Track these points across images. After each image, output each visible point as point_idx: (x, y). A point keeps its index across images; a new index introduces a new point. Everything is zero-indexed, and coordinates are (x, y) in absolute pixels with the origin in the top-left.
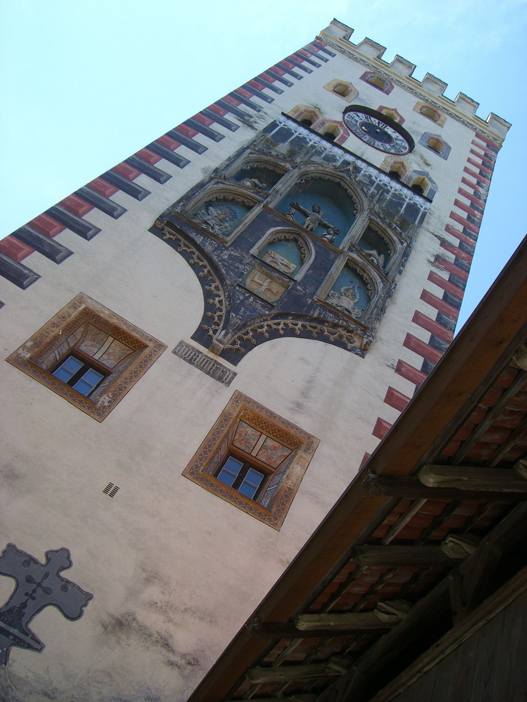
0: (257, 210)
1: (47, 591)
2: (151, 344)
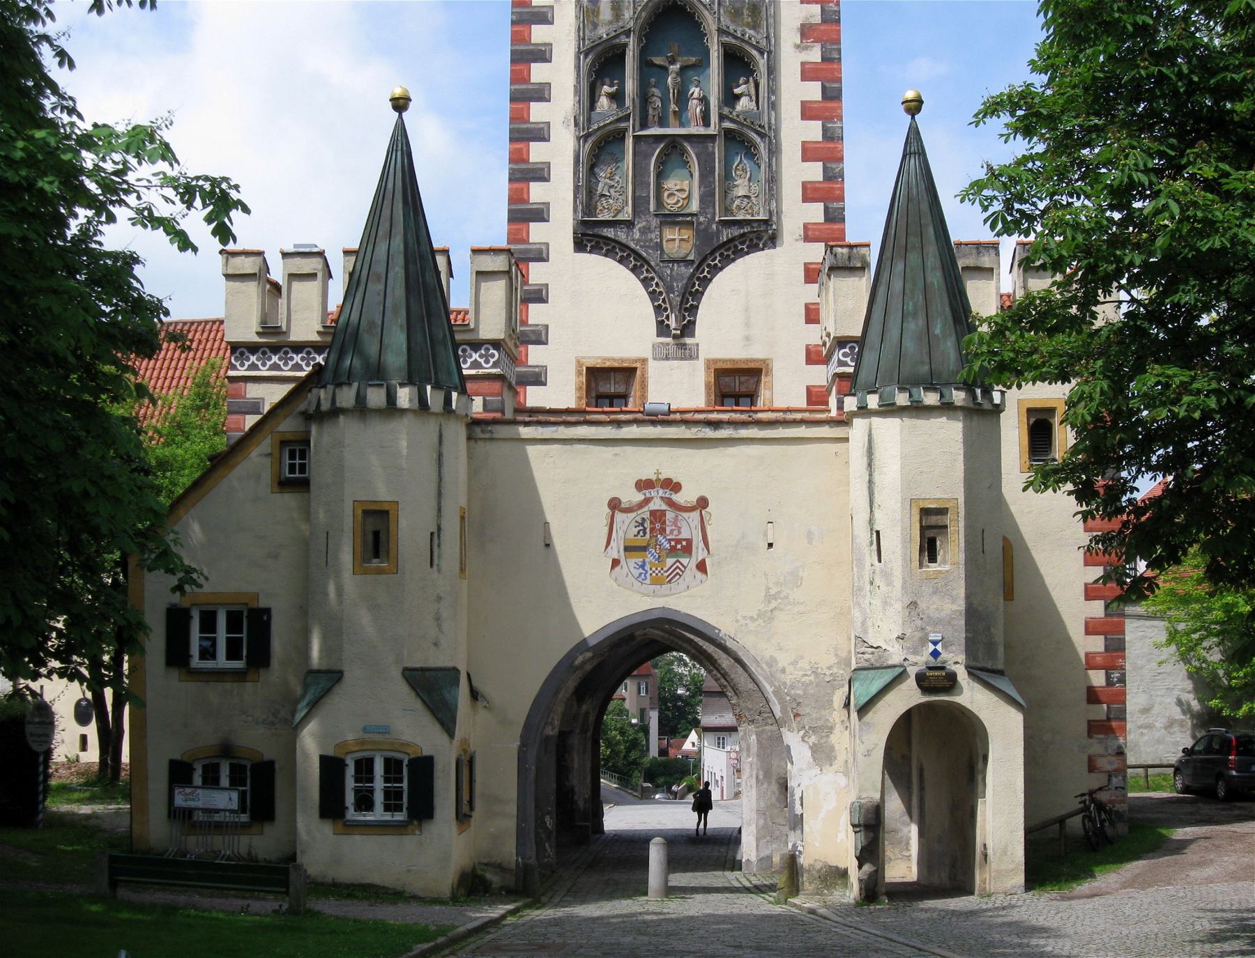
0: (629, 143)
2: (638, 365)
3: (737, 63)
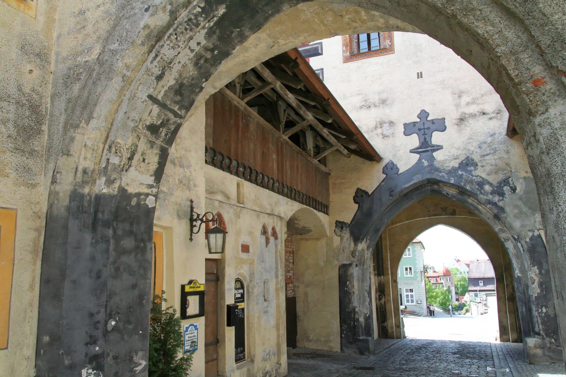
1: (428, 128)
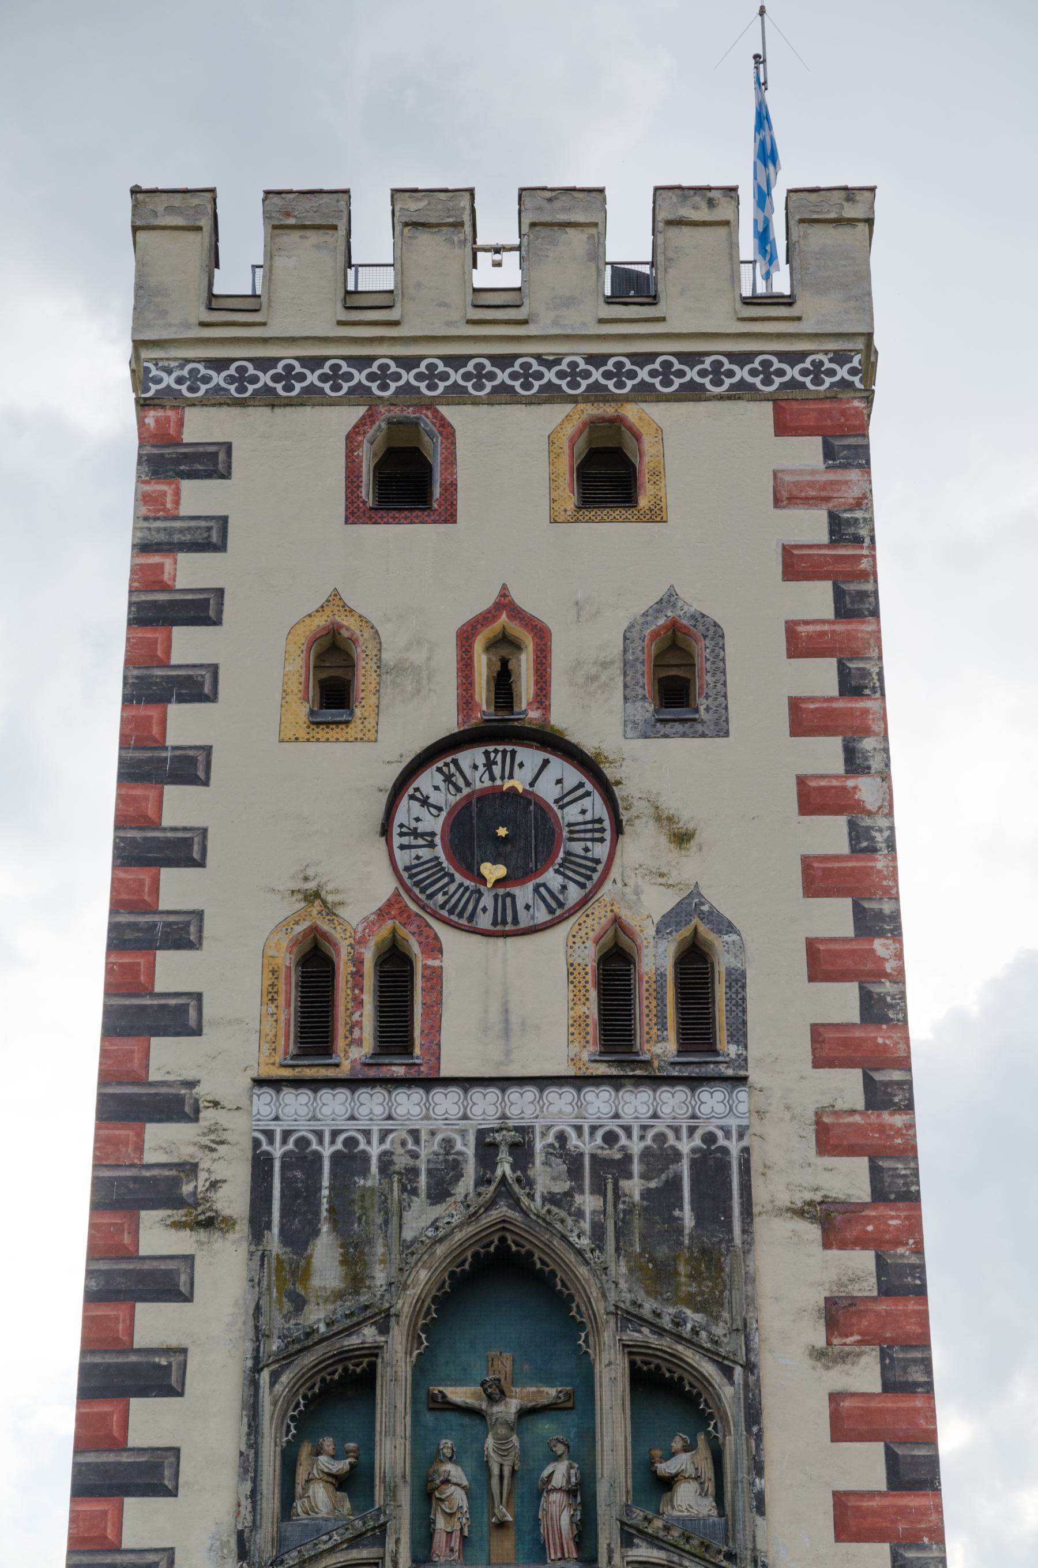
3: (664, 1391)
